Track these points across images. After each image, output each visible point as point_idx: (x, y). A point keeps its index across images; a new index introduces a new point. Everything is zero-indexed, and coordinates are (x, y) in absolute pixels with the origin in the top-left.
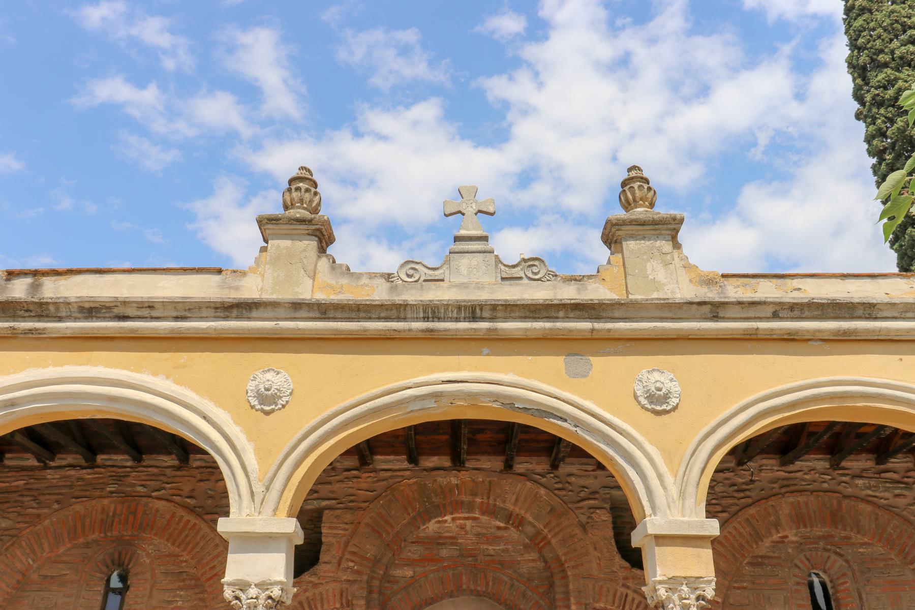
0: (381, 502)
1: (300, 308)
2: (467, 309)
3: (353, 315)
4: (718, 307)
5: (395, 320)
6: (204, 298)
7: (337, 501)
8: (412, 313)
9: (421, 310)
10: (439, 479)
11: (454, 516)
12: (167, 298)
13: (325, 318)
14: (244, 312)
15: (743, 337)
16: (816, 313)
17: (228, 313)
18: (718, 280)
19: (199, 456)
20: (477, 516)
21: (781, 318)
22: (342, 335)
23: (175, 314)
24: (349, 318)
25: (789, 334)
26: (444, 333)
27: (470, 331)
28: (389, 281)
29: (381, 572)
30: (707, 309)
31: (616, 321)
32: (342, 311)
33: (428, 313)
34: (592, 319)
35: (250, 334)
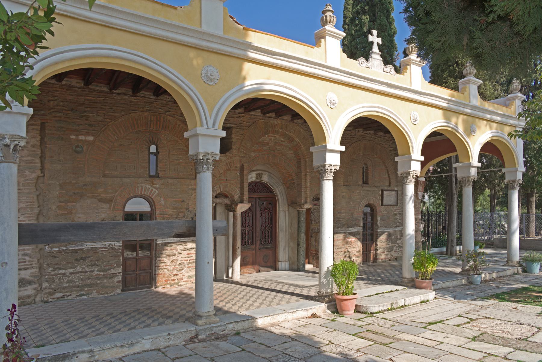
10: (271, 121)
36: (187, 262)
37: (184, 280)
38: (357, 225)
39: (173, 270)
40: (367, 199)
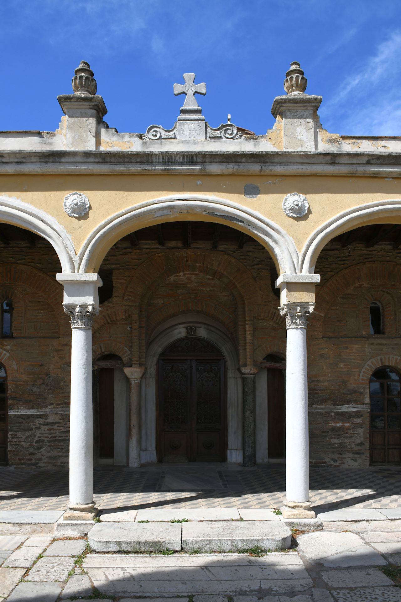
0: (144, 266)
1: (90, 157)
2: (188, 157)
3: (121, 160)
4: (335, 157)
5: (146, 163)
6: (32, 151)
7: (120, 265)
8: (155, 159)
9: (161, 158)
11: (184, 273)
12: (10, 151)
13: (104, 162)
14: (57, 159)
15: (348, 175)
16: (392, 161)
17: (47, 160)
18: (338, 140)
19: (41, 241)
20: (197, 273)
21: (371, 164)
22: (115, 172)
23: (16, 160)
24: (119, 162)
25: (374, 174)
26: (175, 171)
27: (190, 170)
28: (141, 139)
29: (146, 301)
30: (328, 158)
31: (275, 164)
32: (115, 158)
33: (165, 159)
34: (261, 163)
35: (62, 172)
36: (48, 439)
37: (44, 461)
38: (356, 402)
39: (28, 448)
40: (379, 358)
